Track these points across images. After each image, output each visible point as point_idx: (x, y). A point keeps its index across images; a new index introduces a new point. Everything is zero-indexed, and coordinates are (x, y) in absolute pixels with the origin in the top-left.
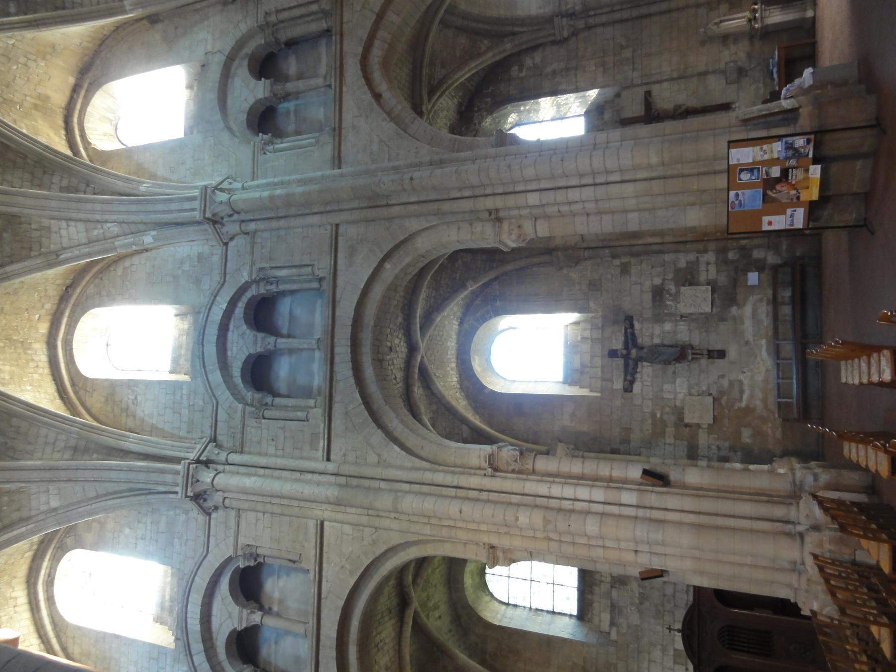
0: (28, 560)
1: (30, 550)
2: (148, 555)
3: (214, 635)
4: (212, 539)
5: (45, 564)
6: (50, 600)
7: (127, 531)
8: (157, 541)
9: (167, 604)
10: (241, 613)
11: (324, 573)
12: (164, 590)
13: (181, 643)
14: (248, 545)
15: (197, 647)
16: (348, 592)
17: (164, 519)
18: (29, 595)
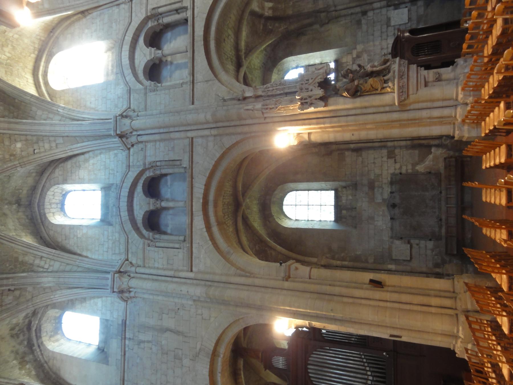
0: (33, 60)
1: (34, 53)
2: (99, 38)
3: (137, 69)
4: (133, 14)
5: (42, 64)
6: (46, 83)
7: (86, 31)
8: (103, 29)
9: (110, 71)
10: (151, 50)
11: (195, 4)
12: (108, 65)
13: (119, 75)
14: (154, 9)
15: (128, 71)
16: (208, 8)
17: (106, 16)
18: (34, 80)
